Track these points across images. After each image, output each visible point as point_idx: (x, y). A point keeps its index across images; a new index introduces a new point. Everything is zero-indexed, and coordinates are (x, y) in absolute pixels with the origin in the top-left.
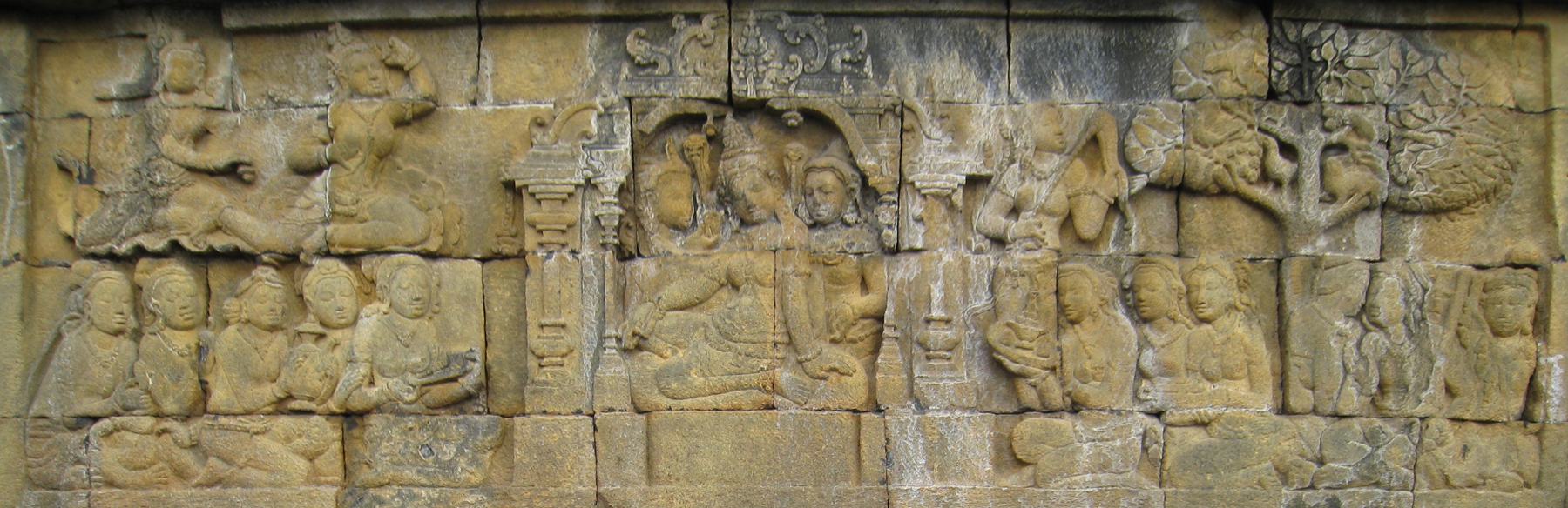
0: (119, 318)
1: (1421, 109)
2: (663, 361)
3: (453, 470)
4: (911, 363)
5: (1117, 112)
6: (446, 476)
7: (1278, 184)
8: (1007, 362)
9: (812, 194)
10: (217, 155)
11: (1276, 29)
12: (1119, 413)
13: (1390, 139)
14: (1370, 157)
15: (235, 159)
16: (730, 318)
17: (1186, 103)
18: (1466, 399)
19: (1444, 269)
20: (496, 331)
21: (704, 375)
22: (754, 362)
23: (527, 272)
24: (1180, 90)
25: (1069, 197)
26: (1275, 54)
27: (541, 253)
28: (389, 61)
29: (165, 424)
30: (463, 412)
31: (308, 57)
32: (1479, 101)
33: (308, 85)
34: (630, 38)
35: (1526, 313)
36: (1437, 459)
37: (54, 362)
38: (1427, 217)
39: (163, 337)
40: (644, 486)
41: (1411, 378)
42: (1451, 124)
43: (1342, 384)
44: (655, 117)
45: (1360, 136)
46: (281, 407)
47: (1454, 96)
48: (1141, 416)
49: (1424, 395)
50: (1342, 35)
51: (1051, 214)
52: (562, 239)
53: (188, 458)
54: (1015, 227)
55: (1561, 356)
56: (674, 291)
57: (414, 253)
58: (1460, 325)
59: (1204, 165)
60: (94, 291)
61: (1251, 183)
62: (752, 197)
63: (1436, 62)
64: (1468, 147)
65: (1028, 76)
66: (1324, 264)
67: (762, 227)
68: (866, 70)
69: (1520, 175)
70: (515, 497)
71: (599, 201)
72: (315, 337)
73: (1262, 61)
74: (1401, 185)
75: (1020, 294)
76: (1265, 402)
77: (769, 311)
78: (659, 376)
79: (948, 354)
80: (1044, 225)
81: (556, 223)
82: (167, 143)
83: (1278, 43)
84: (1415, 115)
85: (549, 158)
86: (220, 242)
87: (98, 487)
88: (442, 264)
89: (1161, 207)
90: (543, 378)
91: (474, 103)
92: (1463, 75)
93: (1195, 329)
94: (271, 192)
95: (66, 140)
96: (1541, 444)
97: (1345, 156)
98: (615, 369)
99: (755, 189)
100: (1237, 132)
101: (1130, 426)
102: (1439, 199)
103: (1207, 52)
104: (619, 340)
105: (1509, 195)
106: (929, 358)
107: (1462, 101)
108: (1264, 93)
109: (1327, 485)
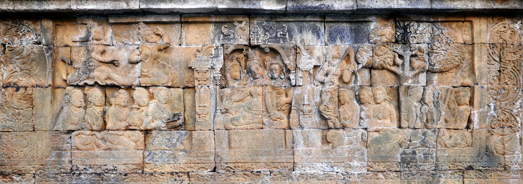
0: (80, 103)
2: (232, 116)
3: (176, 146)
4: (299, 116)
5: (354, 47)
6: (174, 147)
7: (398, 66)
8: (325, 116)
9: (272, 71)
10: (107, 58)
11: (398, 24)
12: (355, 129)
14: (423, 58)
15: (113, 59)
16: (251, 104)
17: (373, 44)
18: (451, 123)
19: (444, 88)
20: (187, 108)
21: (244, 120)
22: (257, 116)
23: (196, 92)
24: (371, 41)
25: (341, 71)
26: (397, 30)
27: (199, 87)
28: (156, 33)
29: (93, 133)
30: (178, 130)
31: (133, 31)
33: (133, 39)
34: (223, 28)
35: (467, 100)
36: (443, 140)
37: (61, 115)
38: (439, 74)
39: (93, 108)
40: (228, 150)
41: (435, 117)
42: (446, 48)
44: (230, 49)
45: (420, 52)
46: (127, 129)
47: (447, 41)
49: (439, 122)
51: (336, 75)
52: (205, 83)
53: (100, 142)
54: (327, 79)
55: (477, 111)
56: (235, 97)
57: (164, 86)
58: (449, 103)
59: (378, 61)
60: (73, 96)
61: (391, 66)
62: (256, 71)
63: (442, 31)
65: (330, 38)
66: (411, 87)
67: (259, 79)
68: (286, 37)
69: (465, 61)
70: (193, 153)
71: (215, 72)
73: (393, 32)
74: (432, 65)
75: (328, 97)
76: (395, 126)
77: (261, 102)
78: (232, 120)
79: (309, 114)
80: (335, 78)
81: (203, 79)
82: (93, 54)
83: (398, 27)
85: (201, 60)
86: (109, 82)
87: (74, 150)
88: (172, 89)
89: (366, 72)
90: (200, 120)
91: (180, 45)
93: (375, 105)
94: (124, 68)
95: (63, 52)
96: (472, 135)
97: (416, 58)
98: (220, 118)
99: (257, 69)
101: (358, 132)
102: (443, 69)
104: (221, 110)
105: (462, 67)
106: (304, 115)
107: (449, 42)
108: (394, 40)
109: (412, 147)
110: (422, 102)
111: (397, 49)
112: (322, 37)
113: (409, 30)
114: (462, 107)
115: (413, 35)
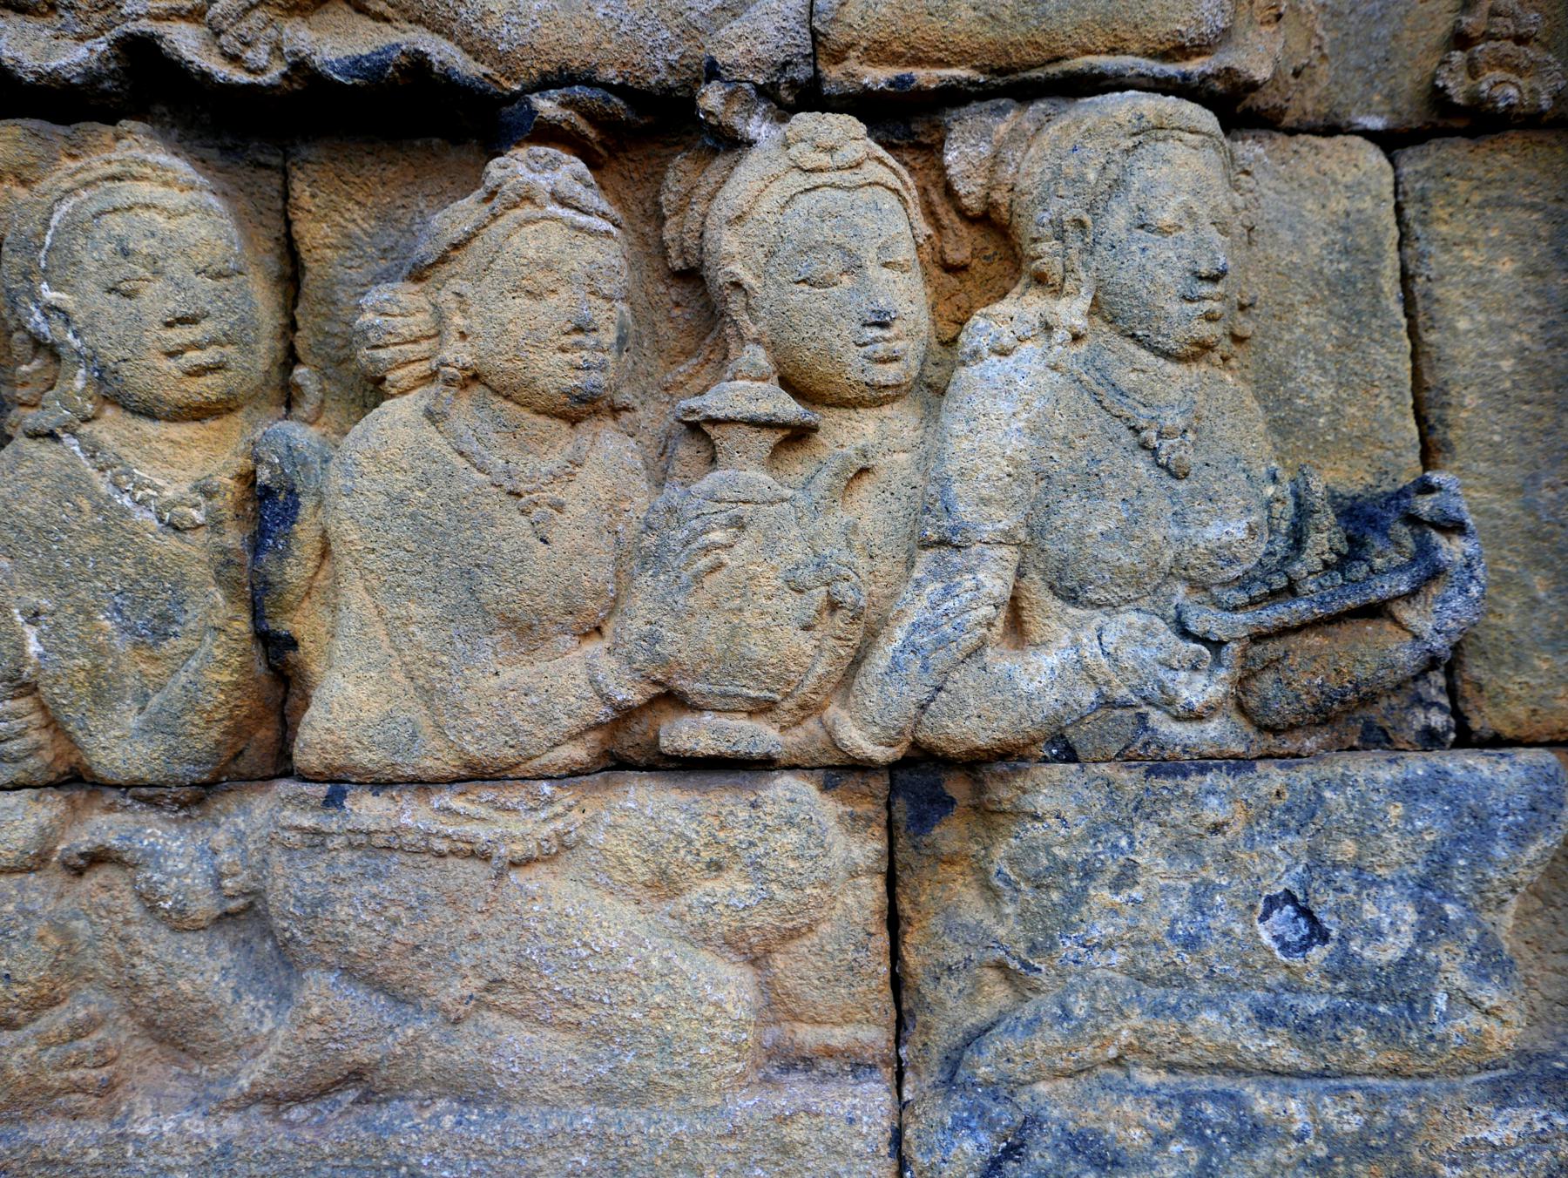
72: (771, 438)
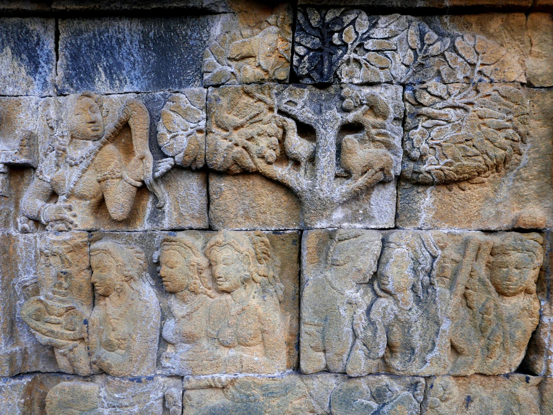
1: (436, 87)
7: (297, 163)
11: (300, 16)
12: (139, 380)
13: (405, 116)
14: (385, 135)
19: (454, 235)
24: (206, 77)
26: (297, 39)
32: (492, 77)
38: (439, 188)
41: (417, 341)
42: (466, 100)
43: (352, 347)
45: (376, 115)
47: (468, 74)
48: (161, 379)
49: (429, 357)
50: (364, 20)
51: (82, 197)
61: (270, 163)
63: (453, 42)
64: (481, 121)
65: (74, 69)
69: (529, 145)
73: (283, 46)
74: (413, 160)
83: (302, 30)
84: (429, 93)
92: (478, 54)
97: (360, 135)
100: (258, 114)
101: (149, 392)
102: (450, 171)
103: (233, 40)
105: (517, 164)
107: (476, 78)
110: (376, 286)
111: (296, 104)
112: (44, 67)
113: (340, 37)
114: (514, 300)
115: (353, 55)
